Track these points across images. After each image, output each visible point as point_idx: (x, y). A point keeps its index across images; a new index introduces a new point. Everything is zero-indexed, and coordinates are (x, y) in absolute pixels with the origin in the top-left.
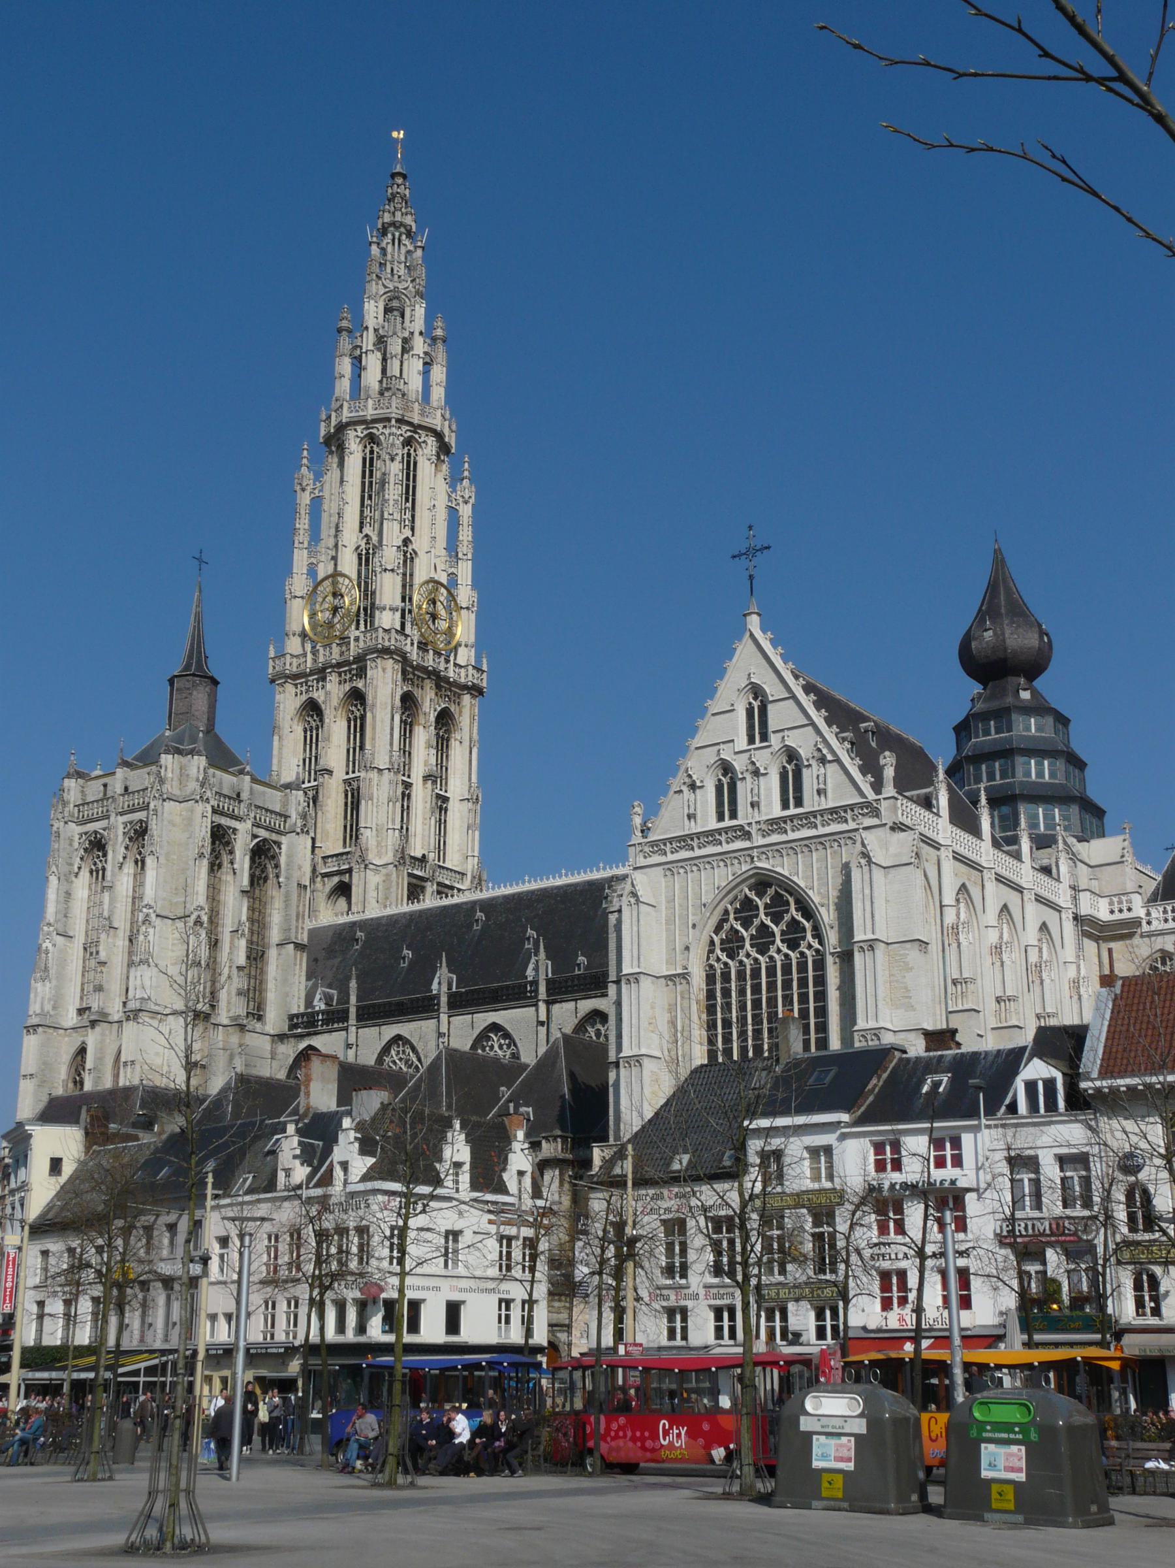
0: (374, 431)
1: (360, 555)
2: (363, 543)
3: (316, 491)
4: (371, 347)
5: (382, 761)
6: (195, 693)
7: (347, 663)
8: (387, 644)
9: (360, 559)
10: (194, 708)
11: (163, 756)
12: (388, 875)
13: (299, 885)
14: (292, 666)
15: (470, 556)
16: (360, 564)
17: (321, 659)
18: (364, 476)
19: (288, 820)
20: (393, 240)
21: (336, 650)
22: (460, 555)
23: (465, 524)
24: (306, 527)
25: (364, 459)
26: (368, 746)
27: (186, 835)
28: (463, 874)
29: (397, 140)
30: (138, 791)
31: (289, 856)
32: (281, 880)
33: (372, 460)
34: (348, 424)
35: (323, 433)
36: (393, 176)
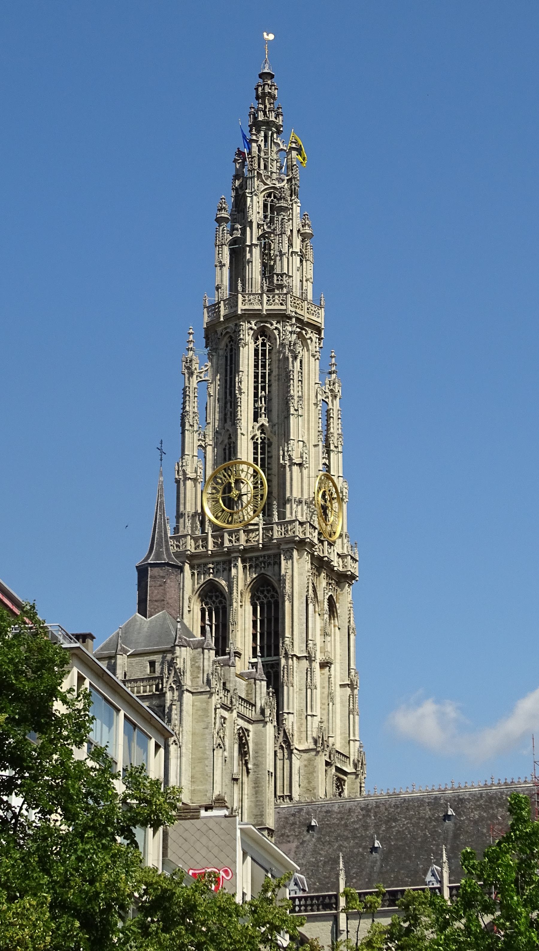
0: (269, 325)
1: (255, 444)
2: (258, 433)
3: (202, 375)
4: (255, 242)
5: (298, 649)
6: (168, 581)
7: (253, 549)
8: (302, 536)
9: (256, 448)
10: (168, 596)
11: (177, 648)
12: (310, 760)
13: (269, 772)
14: (190, 546)
15: (340, 449)
16: (255, 453)
17: (227, 544)
18: (256, 366)
19: (254, 707)
20: (266, 137)
21: (243, 537)
22: (332, 447)
23: (335, 416)
24: (196, 410)
25: (256, 351)
26: (288, 634)
27: (203, 725)
28: (347, 757)
29: (265, 41)
30: (142, 680)
31: (256, 744)
32: (250, 766)
33: (264, 351)
34: (242, 315)
35: (206, 319)
36: (263, 76)
